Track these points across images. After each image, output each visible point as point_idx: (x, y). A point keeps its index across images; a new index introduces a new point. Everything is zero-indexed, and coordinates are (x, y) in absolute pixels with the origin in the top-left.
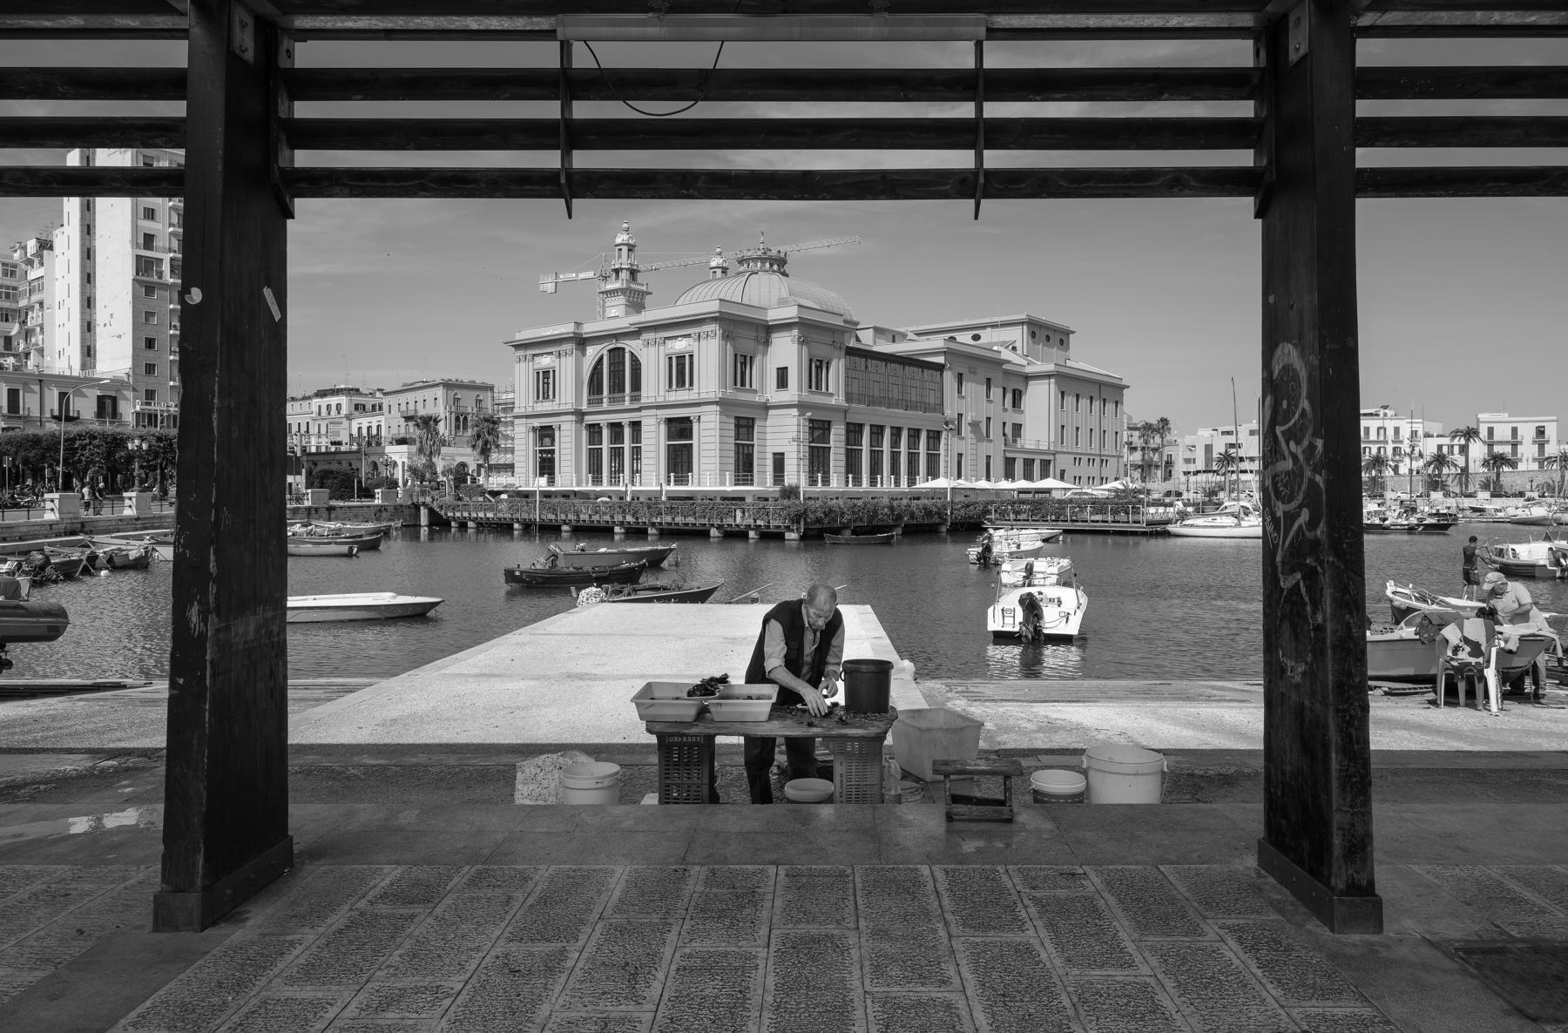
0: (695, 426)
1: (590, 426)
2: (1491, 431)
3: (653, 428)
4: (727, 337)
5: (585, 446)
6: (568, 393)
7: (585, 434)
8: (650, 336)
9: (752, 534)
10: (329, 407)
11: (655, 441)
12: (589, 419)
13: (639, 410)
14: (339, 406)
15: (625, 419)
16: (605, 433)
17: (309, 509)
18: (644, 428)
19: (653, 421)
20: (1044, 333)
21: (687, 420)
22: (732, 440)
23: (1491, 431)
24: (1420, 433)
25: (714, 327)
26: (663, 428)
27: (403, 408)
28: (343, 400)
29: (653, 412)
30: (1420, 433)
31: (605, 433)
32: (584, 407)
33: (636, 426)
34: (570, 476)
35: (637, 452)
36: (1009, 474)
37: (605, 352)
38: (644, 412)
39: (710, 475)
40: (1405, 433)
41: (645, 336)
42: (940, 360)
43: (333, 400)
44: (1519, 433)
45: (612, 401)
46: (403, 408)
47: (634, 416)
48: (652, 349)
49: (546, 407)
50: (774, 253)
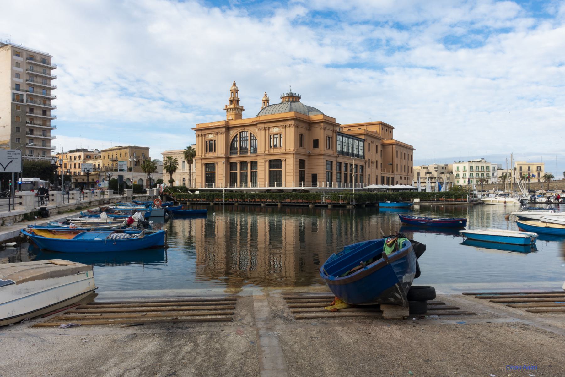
0: (283, 163)
1: (231, 163)
2: (521, 168)
3: (263, 164)
4: (297, 127)
5: (229, 171)
6: (221, 149)
7: (229, 166)
8: (262, 126)
9: (330, 206)
10: (75, 157)
11: (263, 170)
12: (233, 160)
13: (256, 156)
14: (80, 157)
15: (248, 160)
16: (239, 166)
17: (127, 198)
18: (259, 164)
19: (263, 161)
20: (386, 128)
21: (280, 161)
22: (299, 169)
23: (521, 168)
24: (496, 169)
25: (292, 122)
26: (268, 164)
27: (110, 157)
28: (82, 154)
29: (263, 157)
30: (496, 169)
31: (239, 166)
32: (229, 156)
33: (254, 164)
34: (221, 183)
35: (254, 176)
36: (383, 183)
37: (239, 133)
38: (258, 157)
39: (290, 183)
40: (491, 169)
41: (259, 126)
42: (363, 137)
43: (77, 154)
44: (531, 168)
45: (240, 153)
46: (110, 157)
47: (253, 159)
48: (263, 132)
49: (211, 155)
50: (297, 95)
